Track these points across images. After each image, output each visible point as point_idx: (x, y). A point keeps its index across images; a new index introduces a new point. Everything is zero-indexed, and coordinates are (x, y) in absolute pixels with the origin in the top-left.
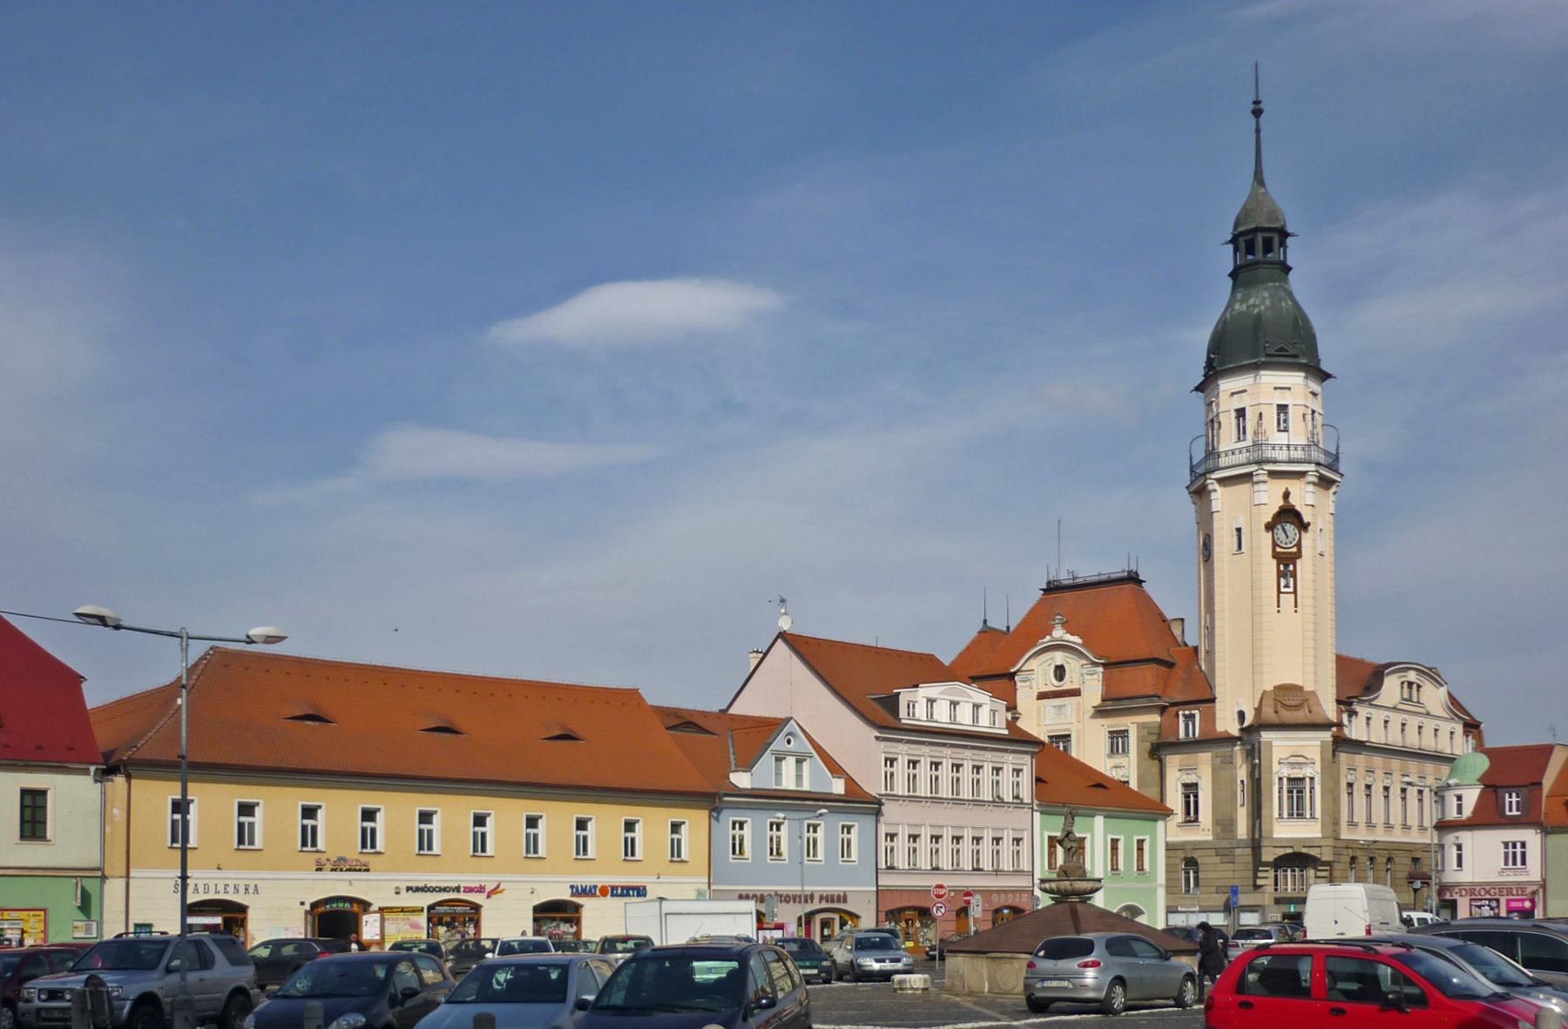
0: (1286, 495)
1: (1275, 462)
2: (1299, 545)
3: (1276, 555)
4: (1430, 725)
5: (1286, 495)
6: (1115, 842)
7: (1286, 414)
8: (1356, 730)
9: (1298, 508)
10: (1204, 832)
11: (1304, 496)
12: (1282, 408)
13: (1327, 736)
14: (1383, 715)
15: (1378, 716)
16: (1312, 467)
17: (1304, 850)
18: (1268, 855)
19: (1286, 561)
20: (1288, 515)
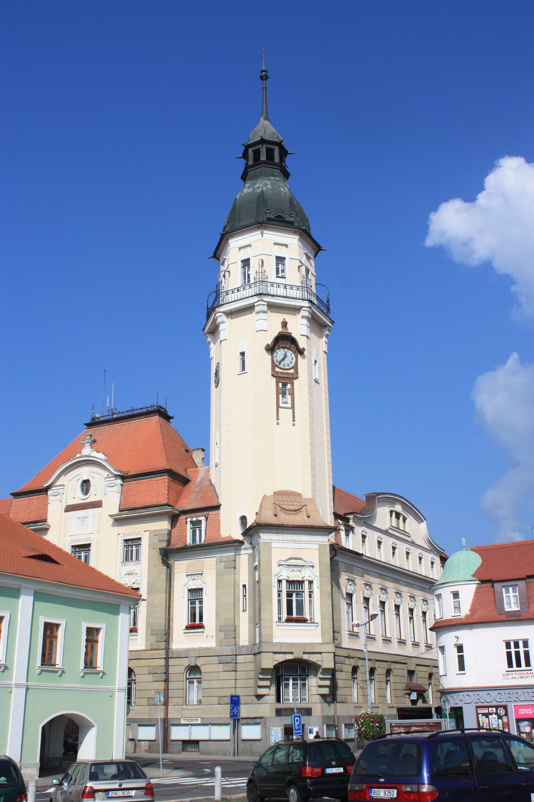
0: (284, 324)
4: (415, 552)
5: (284, 324)
6: (50, 629)
8: (351, 542)
9: (293, 335)
10: (207, 640)
11: (298, 327)
12: (280, 260)
13: (326, 540)
14: (376, 535)
15: (373, 536)
17: (306, 657)
18: (269, 662)
19: (285, 380)
20: (284, 340)
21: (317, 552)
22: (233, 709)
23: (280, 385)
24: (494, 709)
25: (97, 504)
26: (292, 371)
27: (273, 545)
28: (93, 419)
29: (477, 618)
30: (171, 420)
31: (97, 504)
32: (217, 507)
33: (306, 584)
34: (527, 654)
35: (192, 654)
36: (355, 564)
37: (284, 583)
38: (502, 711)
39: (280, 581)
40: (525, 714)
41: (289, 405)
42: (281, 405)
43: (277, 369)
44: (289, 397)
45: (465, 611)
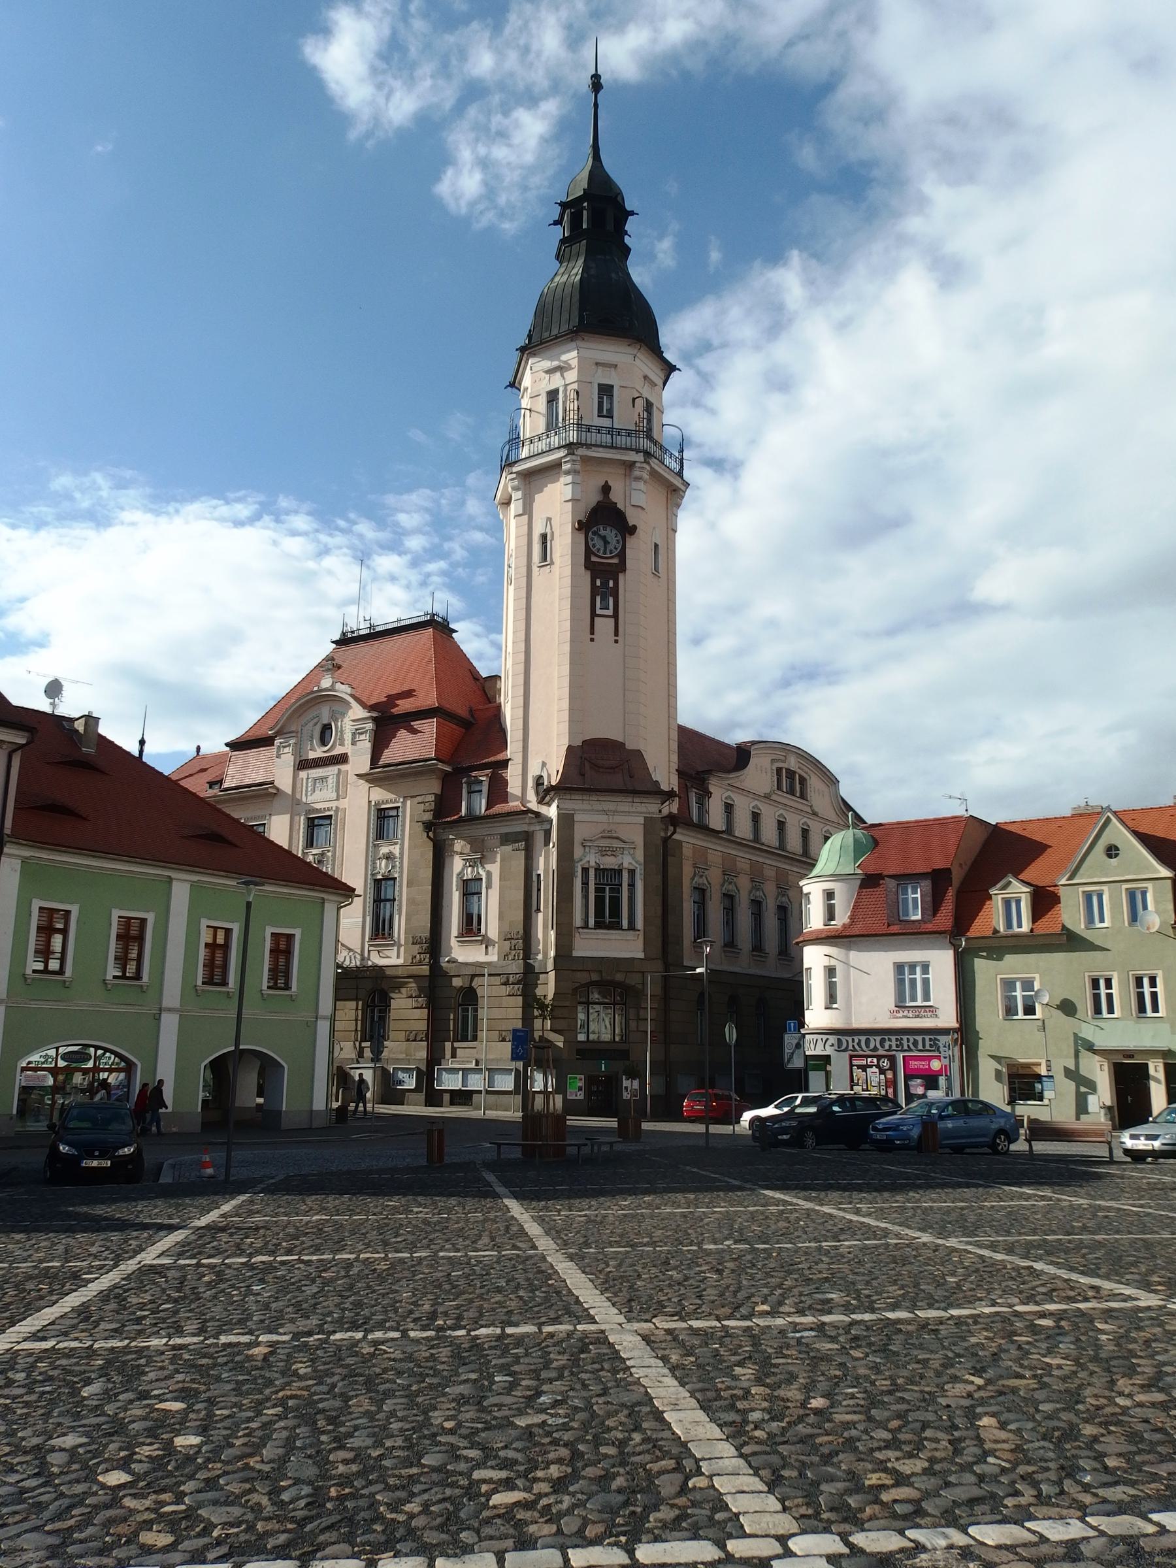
1: (589, 446)
2: (622, 555)
3: (589, 565)
5: (606, 489)
7: (611, 396)
16: (640, 457)
21: (641, 829)
22: (517, 1048)
23: (598, 583)
24: (875, 1060)
25: (342, 759)
26: (615, 561)
27: (577, 818)
28: (344, 634)
29: (856, 930)
30: (454, 635)
31: (342, 759)
32: (504, 764)
33: (625, 875)
34: (926, 982)
35: (469, 971)
36: (709, 845)
37: (592, 873)
38: (885, 1064)
39: (585, 870)
40: (919, 1069)
41: (610, 612)
42: (598, 612)
43: (594, 559)
44: (611, 600)
45: (842, 918)
